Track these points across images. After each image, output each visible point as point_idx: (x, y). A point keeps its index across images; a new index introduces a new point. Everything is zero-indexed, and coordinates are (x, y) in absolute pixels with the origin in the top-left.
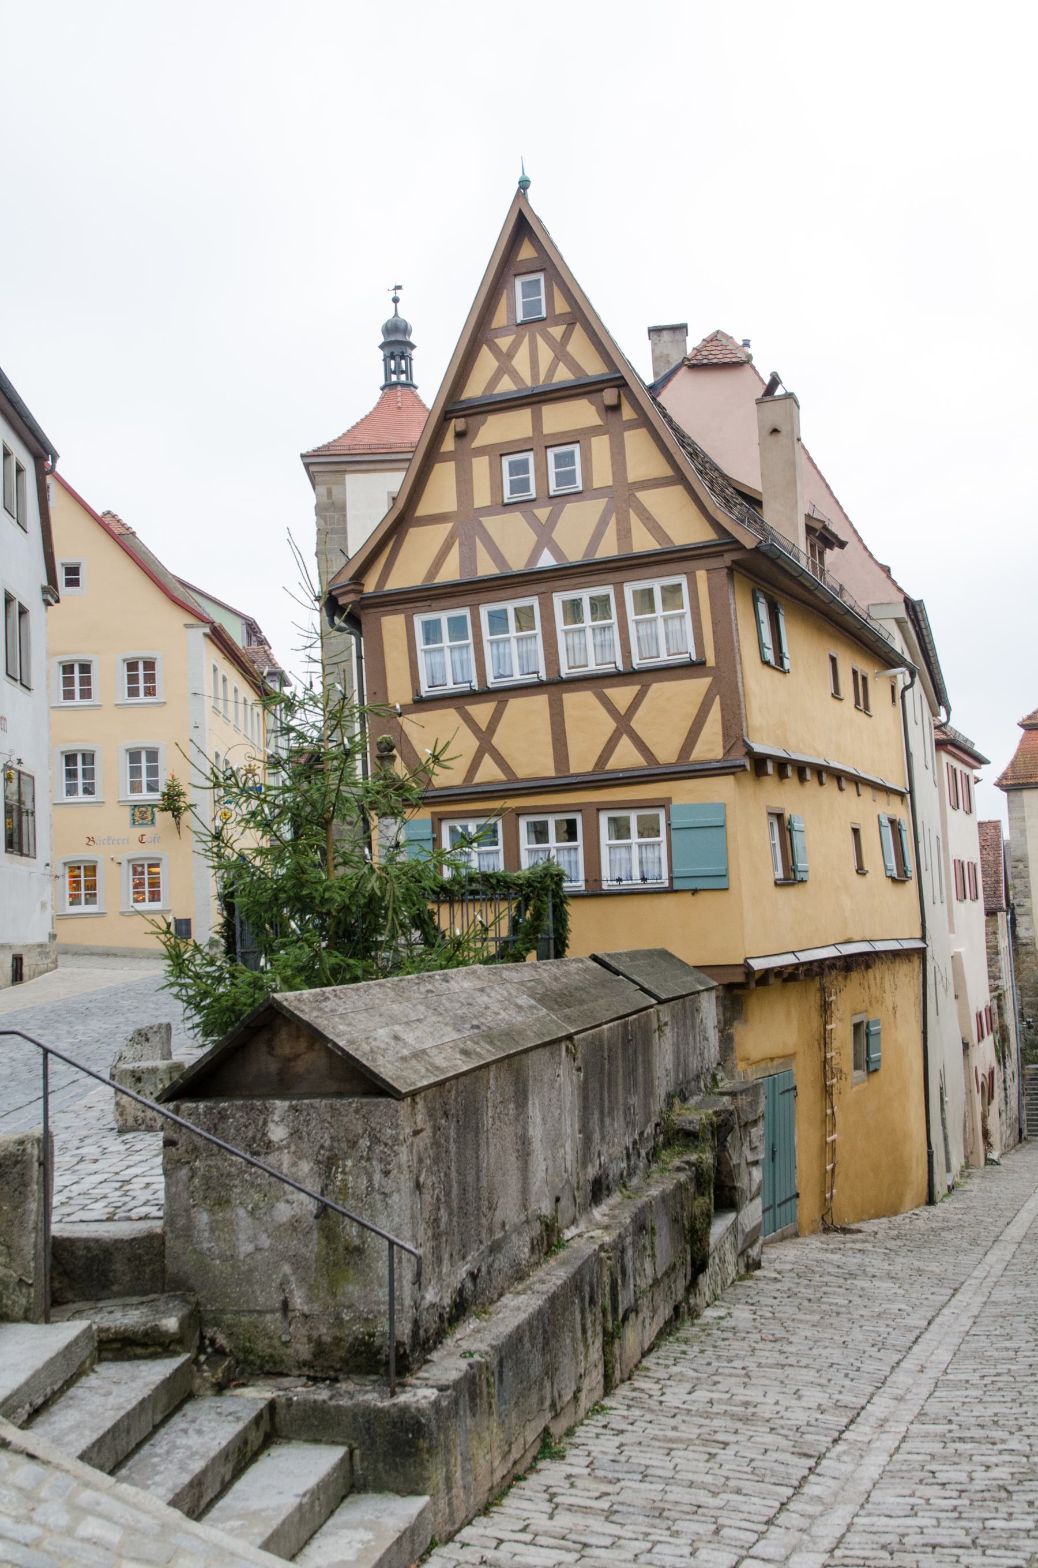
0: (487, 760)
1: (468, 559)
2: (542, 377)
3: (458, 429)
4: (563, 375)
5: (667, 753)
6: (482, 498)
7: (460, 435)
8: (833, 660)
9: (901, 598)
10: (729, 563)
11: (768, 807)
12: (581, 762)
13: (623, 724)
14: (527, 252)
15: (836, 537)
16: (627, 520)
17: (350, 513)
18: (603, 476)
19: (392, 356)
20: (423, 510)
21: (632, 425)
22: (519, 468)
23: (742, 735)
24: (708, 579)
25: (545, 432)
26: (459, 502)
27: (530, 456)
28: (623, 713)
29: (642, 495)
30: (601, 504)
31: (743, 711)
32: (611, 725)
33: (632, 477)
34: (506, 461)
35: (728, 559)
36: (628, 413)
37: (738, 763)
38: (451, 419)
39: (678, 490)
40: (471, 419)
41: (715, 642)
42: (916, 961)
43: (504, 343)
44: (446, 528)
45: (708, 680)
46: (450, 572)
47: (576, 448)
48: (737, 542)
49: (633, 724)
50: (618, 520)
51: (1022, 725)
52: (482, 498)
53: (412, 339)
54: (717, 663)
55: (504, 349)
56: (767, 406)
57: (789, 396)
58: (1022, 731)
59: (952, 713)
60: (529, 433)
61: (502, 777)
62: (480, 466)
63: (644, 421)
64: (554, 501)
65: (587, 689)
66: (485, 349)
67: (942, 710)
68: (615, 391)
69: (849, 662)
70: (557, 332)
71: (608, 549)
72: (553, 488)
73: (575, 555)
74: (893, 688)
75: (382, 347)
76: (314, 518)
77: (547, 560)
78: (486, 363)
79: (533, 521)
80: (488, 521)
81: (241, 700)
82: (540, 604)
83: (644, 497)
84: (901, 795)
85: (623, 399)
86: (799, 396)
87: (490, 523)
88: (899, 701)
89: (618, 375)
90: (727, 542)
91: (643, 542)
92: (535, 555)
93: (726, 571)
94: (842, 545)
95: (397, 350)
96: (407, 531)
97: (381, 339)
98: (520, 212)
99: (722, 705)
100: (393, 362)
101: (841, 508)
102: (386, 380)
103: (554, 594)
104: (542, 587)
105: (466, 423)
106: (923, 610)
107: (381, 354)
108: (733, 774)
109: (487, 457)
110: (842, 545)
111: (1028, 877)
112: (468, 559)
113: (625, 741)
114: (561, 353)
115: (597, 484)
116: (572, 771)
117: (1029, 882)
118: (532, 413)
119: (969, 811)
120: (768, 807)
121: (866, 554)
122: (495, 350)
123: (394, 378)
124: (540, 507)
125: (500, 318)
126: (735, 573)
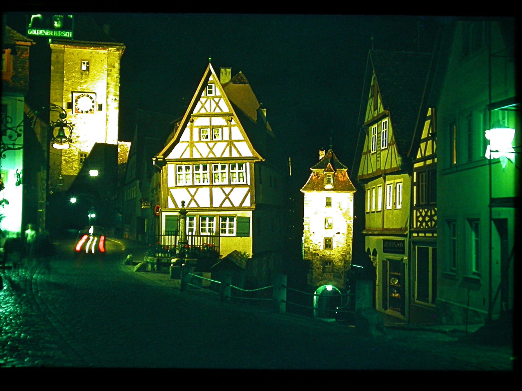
0: (193, 201)
2: (212, 110)
4: (218, 111)
12: (216, 204)
13: (227, 197)
18: (226, 138)
21: (234, 126)
29: (235, 143)
32: (225, 197)
33: (233, 138)
36: (233, 122)
43: (202, 100)
46: (187, 156)
48: (257, 157)
49: (230, 197)
61: (196, 206)
65: (219, 187)
70: (217, 100)
71: (226, 155)
73: (218, 155)
77: (211, 156)
78: (199, 105)
91: (235, 154)
98: (210, 69)
99: (251, 195)
113: (227, 200)
115: (225, 139)
116: (214, 206)
125: (203, 94)
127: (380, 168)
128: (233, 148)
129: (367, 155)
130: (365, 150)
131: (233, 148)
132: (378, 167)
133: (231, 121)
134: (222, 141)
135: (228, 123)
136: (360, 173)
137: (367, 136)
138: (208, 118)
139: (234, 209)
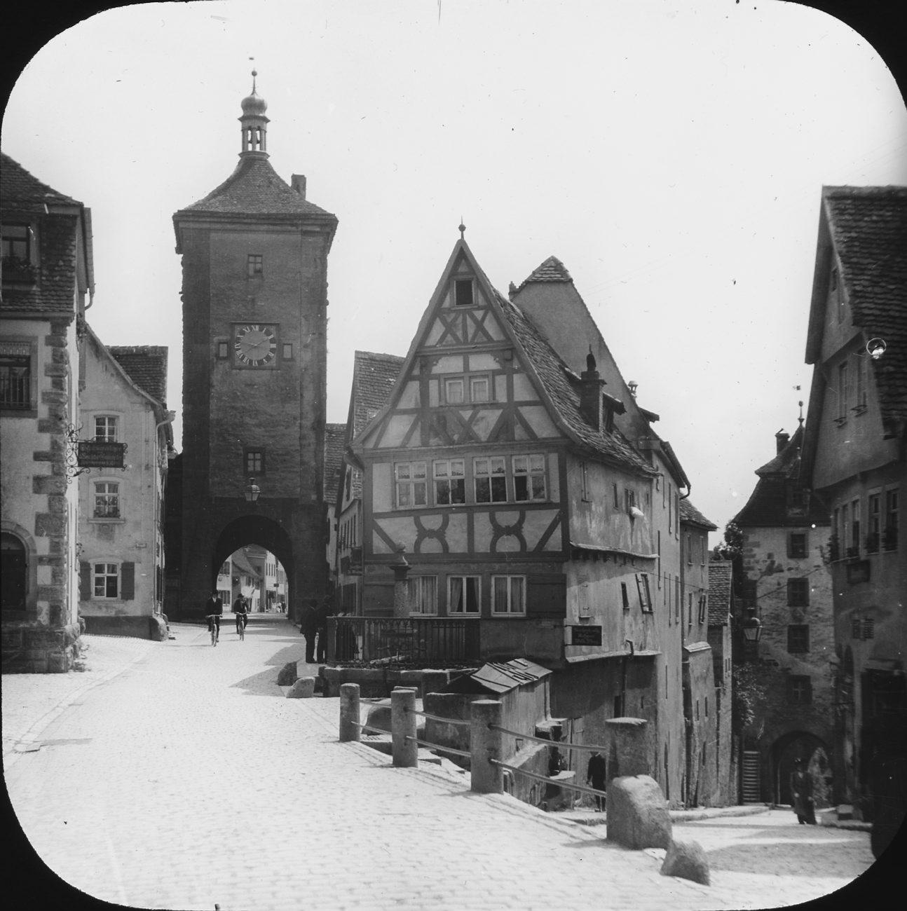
7: (421, 368)
14: (463, 269)
18: (502, 398)
19: (250, 128)
21: (517, 372)
51: (758, 473)
53: (267, 114)
55: (449, 320)
58: (758, 478)
62: (433, 385)
63: (524, 368)
68: (510, 352)
70: (479, 314)
75: (240, 119)
83: (526, 411)
85: (514, 356)
95: (256, 124)
97: (241, 113)
100: (249, 132)
102: (243, 148)
107: (240, 124)
114: (480, 325)
118: (464, 358)
122: (444, 322)
123: (250, 147)
125: (447, 303)
133: (511, 360)
134: (494, 405)
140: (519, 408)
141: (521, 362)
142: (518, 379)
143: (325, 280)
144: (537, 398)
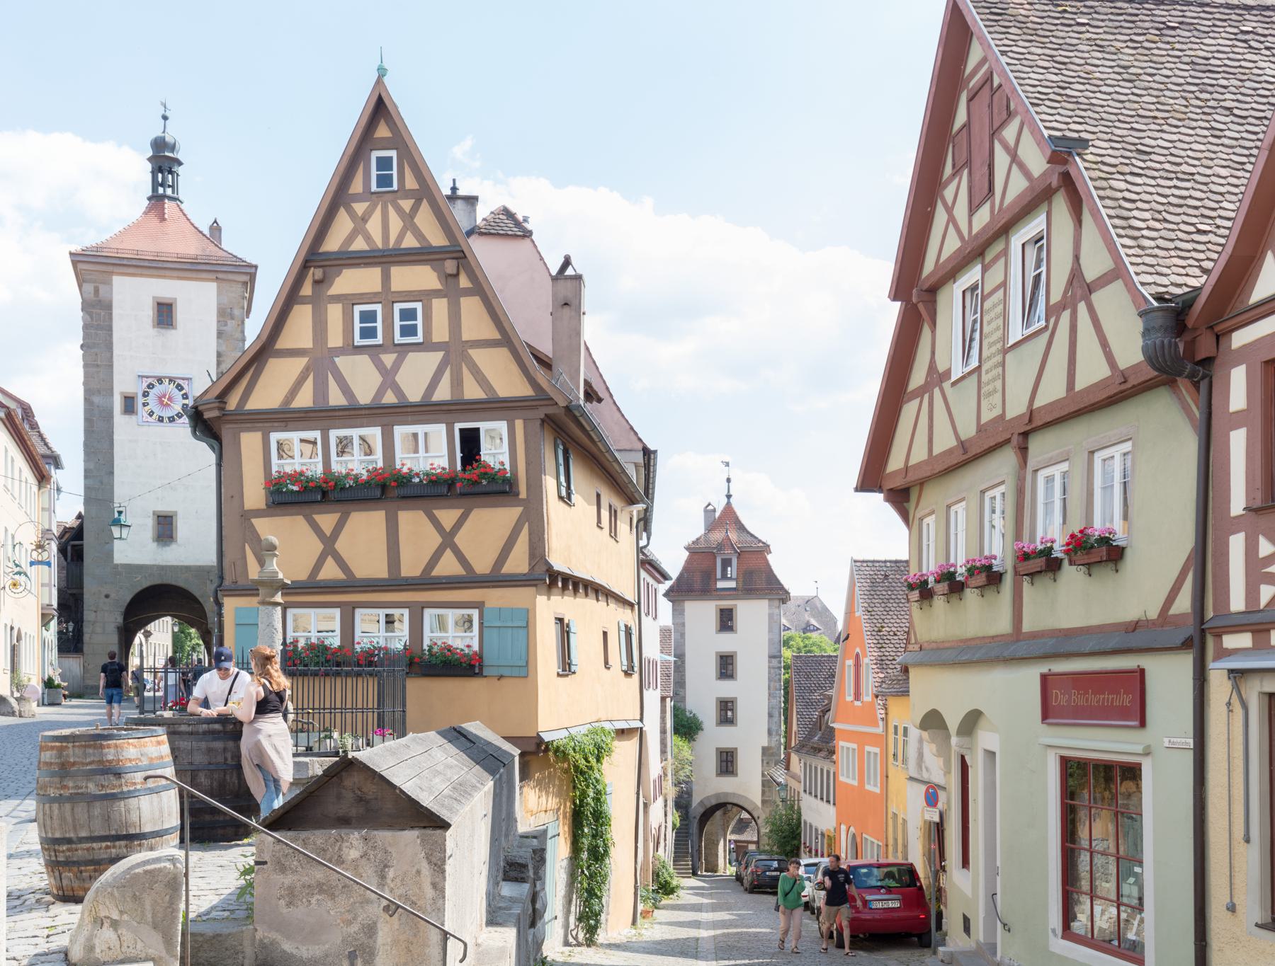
1: (321, 390)
3: (316, 278)
5: (482, 566)
6: (335, 340)
7: (317, 283)
8: (598, 496)
9: (640, 446)
10: (543, 416)
11: (555, 613)
13: (448, 540)
15: (596, 393)
16: (461, 368)
17: (115, 312)
18: (441, 333)
20: (283, 343)
21: (467, 292)
22: (368, 317)
23: (545, 555)
24: (525, 427)
25: (393, 289)
26: (315, 341)
27: (378, 308)
28: (448, 530)
29: (473, 353)
30: (440, 355)
31: (546, 536)
33: (466, 336)
34: (358, 309)
35: (541, 413)
36: (464, 282)
37: (540, 577)
38: (310, 267)
39: (504, 352)
40: (327, 269)
41: (527, 479)
42: (635, 741)
44: (302, 362)
45: (519, 510)
47: (418, 306)
48: (552, 399)
50: (451, 369)
52: (335, 340)
54: (528, 495)
56: (561, 283)
57: (578, 278)
59: (652, 538)
60: (378, 288)
62: (334, 313)
64: (399, 348)
66: (342, 215)
67: (644, 535)
68: (454, 262)
69: (608, 498)
71: (443, 393)
72: (398, 339)
73: (415, 395)
74: (631, 519)
76: (81, 314)
77: (390, 398)
79: (380, 366)
80: (340, 361)
81: (23, 479)
82: (382, 434)
83: (477, 355)
84: (631, 605)
86: (585, 278)
87: (340, 361)
88: (634, 530)
89: (458, 249)
90: (542, 398)
91: (472, 391)
92: (380, 392)
93: (539, 422)
94: (600, 400)
96: (267, 361)
101: (597, 368)
103: (395, 427)
104: (385, 420)
105: (324, 273)
106: (655, 458)
108: (535, 585)
109: (341, 305)
110: (600, 400)
111: (684, 671)
112: (321, 390)
113: (448, 555)
117: (684, 675)
119: (655, 618)
120: (555, 613)
121: (615, 408)
124: (386, 352)
126: (545, 424)
127: (1003, 416)
128: (465, 371)
129: (926, 397)
130: (918, 377)
131: (465, 371)
132: (987, 416)
133: (457, 275)
135: (446, 284)
136: (895, 462)
137: (926, 331)
138: (376, 273)
139: (471, 580)
140: (471, 352)
141: (473, 276)
142: (471, 307)
143: (243, 332)
144: (498, 336)
